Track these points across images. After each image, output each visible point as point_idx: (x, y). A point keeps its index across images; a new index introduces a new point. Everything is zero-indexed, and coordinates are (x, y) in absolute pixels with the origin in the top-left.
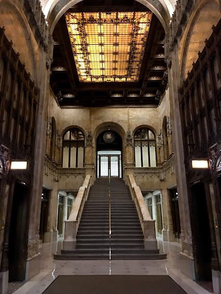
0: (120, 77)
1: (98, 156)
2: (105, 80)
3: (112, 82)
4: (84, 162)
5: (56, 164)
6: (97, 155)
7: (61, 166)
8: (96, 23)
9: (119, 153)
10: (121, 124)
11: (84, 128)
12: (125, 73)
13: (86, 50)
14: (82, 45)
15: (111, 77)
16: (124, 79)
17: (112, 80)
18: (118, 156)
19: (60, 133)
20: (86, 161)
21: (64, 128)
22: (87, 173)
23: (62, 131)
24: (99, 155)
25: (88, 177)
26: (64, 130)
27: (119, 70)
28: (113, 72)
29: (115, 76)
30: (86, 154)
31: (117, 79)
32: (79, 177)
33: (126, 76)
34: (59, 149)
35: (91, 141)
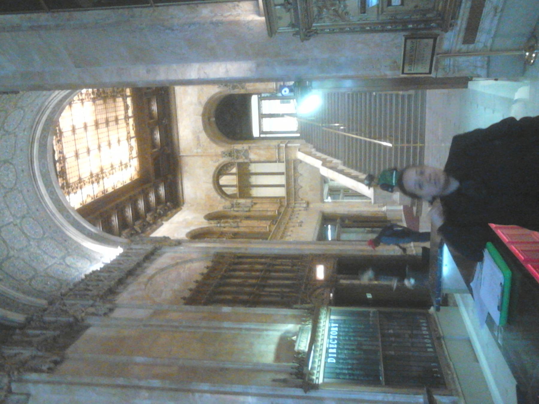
0: (126, 108)
1: (262, 136)
2: (132, 134)
3: (134, 121)
4: (275, 162)
5: (280, 207)
6: (260, 139)
7: (282, 200)
8: (64, 166)
9: (254, 99)
10: (205, 99)
11: (217, 164)
12: (120, 100)
13: (97, 175)
14: (93, 183)
15: (128, 124)
16: (129, 101)
17: (131, 121)
18: (261, 99)
19: (228, 203)
20: (274, 159)
21: (219, 197)
22: (293, 158)
23: (223, 200)
24: (260, 134)
25: (300, 156)
26: (222, 197)
27: (118, 113)
28: (122, 124)
29: (127, 118)
30: (263, 159)
31: (130, 113)
32: (301, 169)
33: (124, 98)
34: (255, 204)
35: (237, 151)
